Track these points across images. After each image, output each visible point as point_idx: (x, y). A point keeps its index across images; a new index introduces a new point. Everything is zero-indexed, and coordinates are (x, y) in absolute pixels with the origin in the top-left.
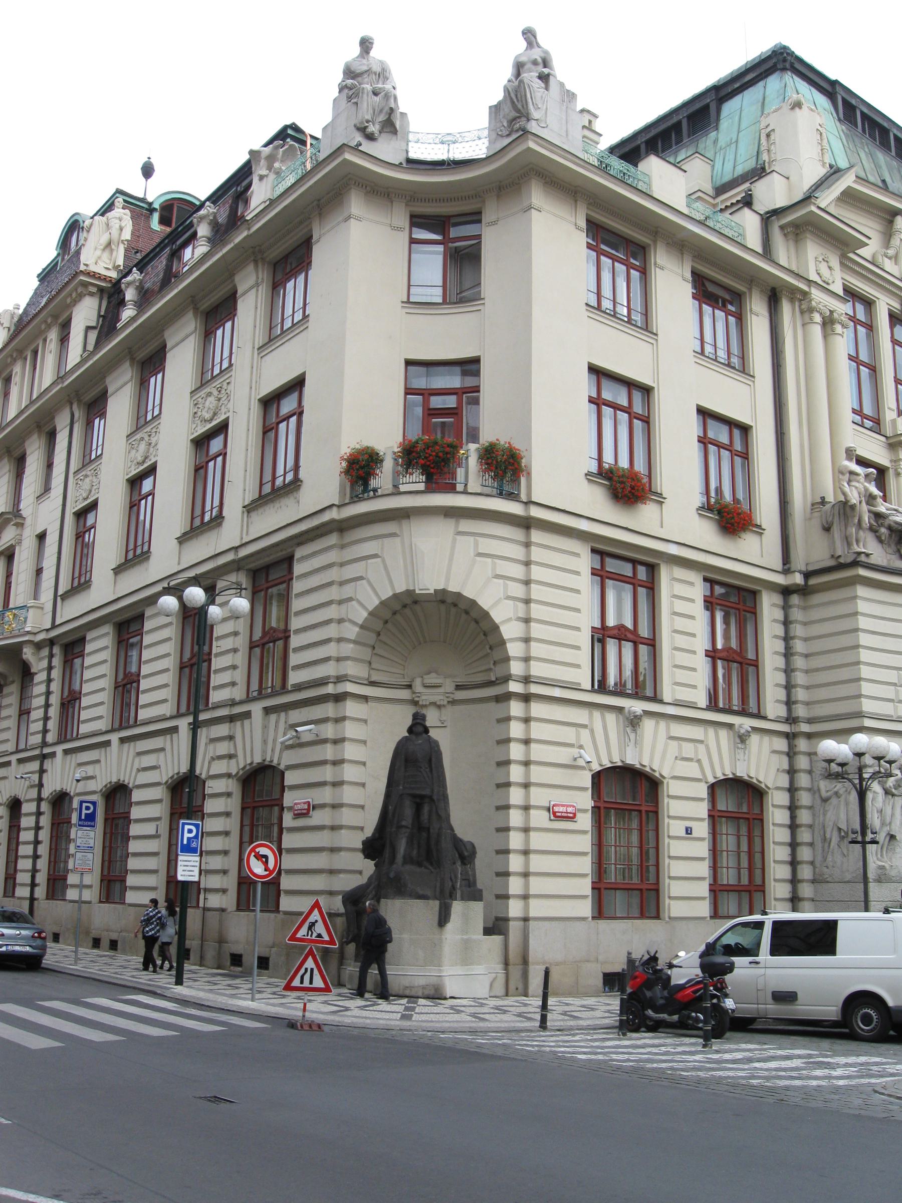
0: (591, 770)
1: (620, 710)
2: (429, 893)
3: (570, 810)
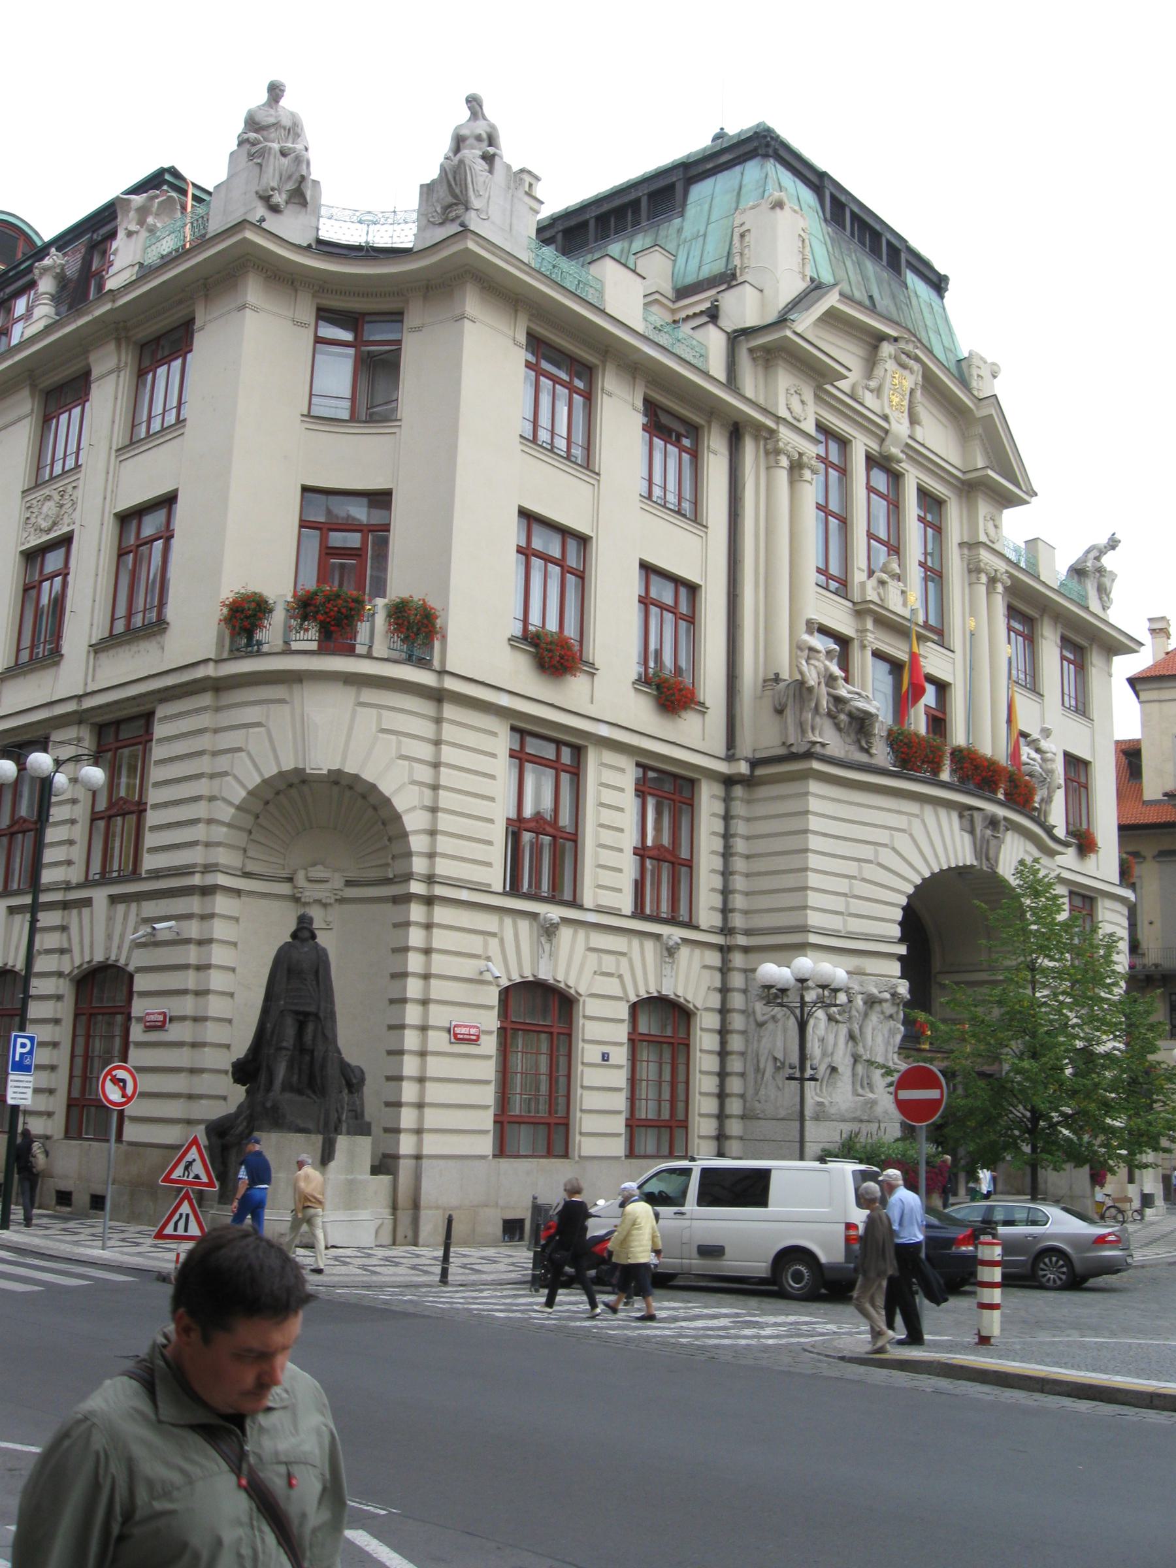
0: (498, 986)
1: (534, 916)
2: (311, 1126)
3: (473, 1031)
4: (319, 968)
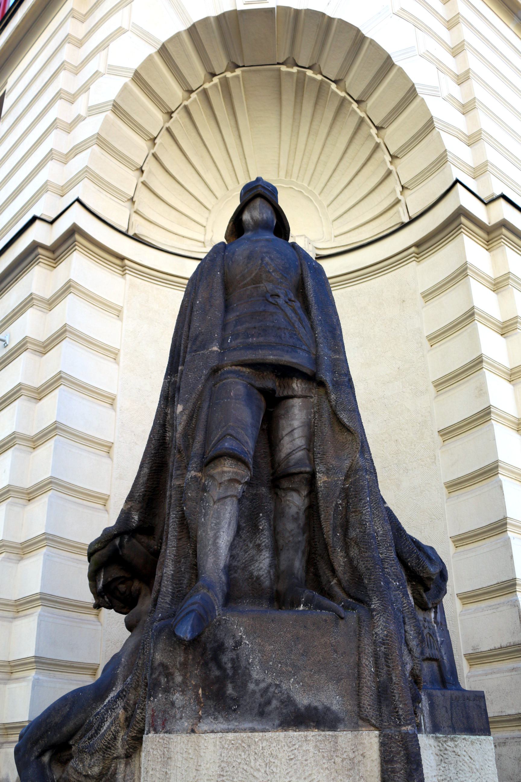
2: (332, 699)
4: (306, 289)
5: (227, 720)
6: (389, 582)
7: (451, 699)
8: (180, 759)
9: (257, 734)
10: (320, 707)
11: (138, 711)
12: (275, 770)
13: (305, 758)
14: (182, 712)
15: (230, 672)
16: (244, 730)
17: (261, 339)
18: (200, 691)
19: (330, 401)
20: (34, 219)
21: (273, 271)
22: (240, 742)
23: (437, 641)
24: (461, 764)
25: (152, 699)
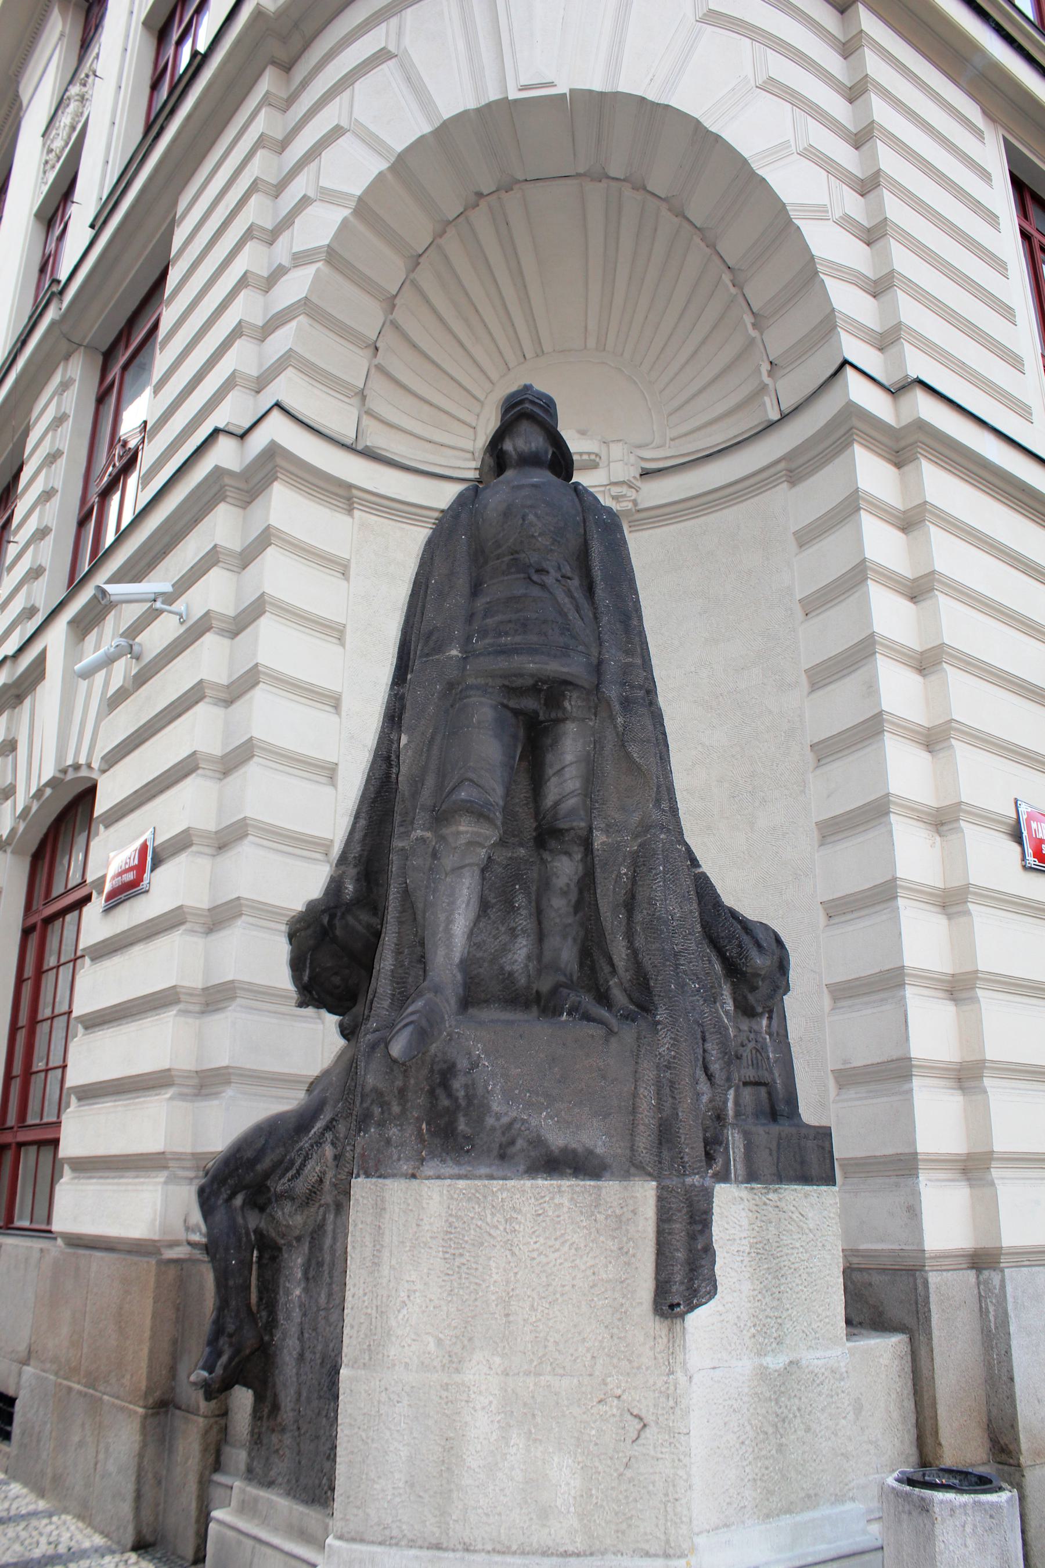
5: (458, 1163)
6: (684, 985)
7: (780, 1138)
8: (397, 1210)
9: (495, 1182)
10: (580, 1150)
11: (348, 1148)
12: (517, 1227)
13: (557, 1213)
14: (400, 1152)
15: (463, 1103)
16: (480, 1177)
17: (518, 639)
18: (424, 1126)
19: (615, 727)
20: (216, 432)
21: (540, 535)
22: (473, 1191)
23: (768, 1058)
24: (786, 1223)
25: (362, 1134)
